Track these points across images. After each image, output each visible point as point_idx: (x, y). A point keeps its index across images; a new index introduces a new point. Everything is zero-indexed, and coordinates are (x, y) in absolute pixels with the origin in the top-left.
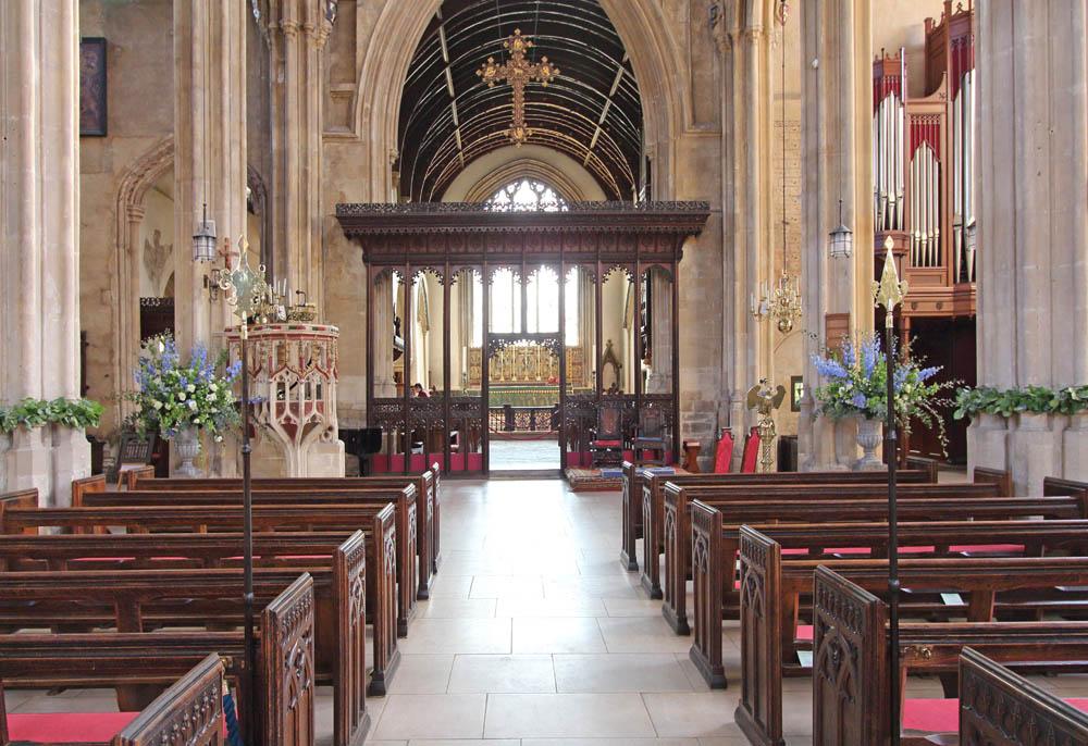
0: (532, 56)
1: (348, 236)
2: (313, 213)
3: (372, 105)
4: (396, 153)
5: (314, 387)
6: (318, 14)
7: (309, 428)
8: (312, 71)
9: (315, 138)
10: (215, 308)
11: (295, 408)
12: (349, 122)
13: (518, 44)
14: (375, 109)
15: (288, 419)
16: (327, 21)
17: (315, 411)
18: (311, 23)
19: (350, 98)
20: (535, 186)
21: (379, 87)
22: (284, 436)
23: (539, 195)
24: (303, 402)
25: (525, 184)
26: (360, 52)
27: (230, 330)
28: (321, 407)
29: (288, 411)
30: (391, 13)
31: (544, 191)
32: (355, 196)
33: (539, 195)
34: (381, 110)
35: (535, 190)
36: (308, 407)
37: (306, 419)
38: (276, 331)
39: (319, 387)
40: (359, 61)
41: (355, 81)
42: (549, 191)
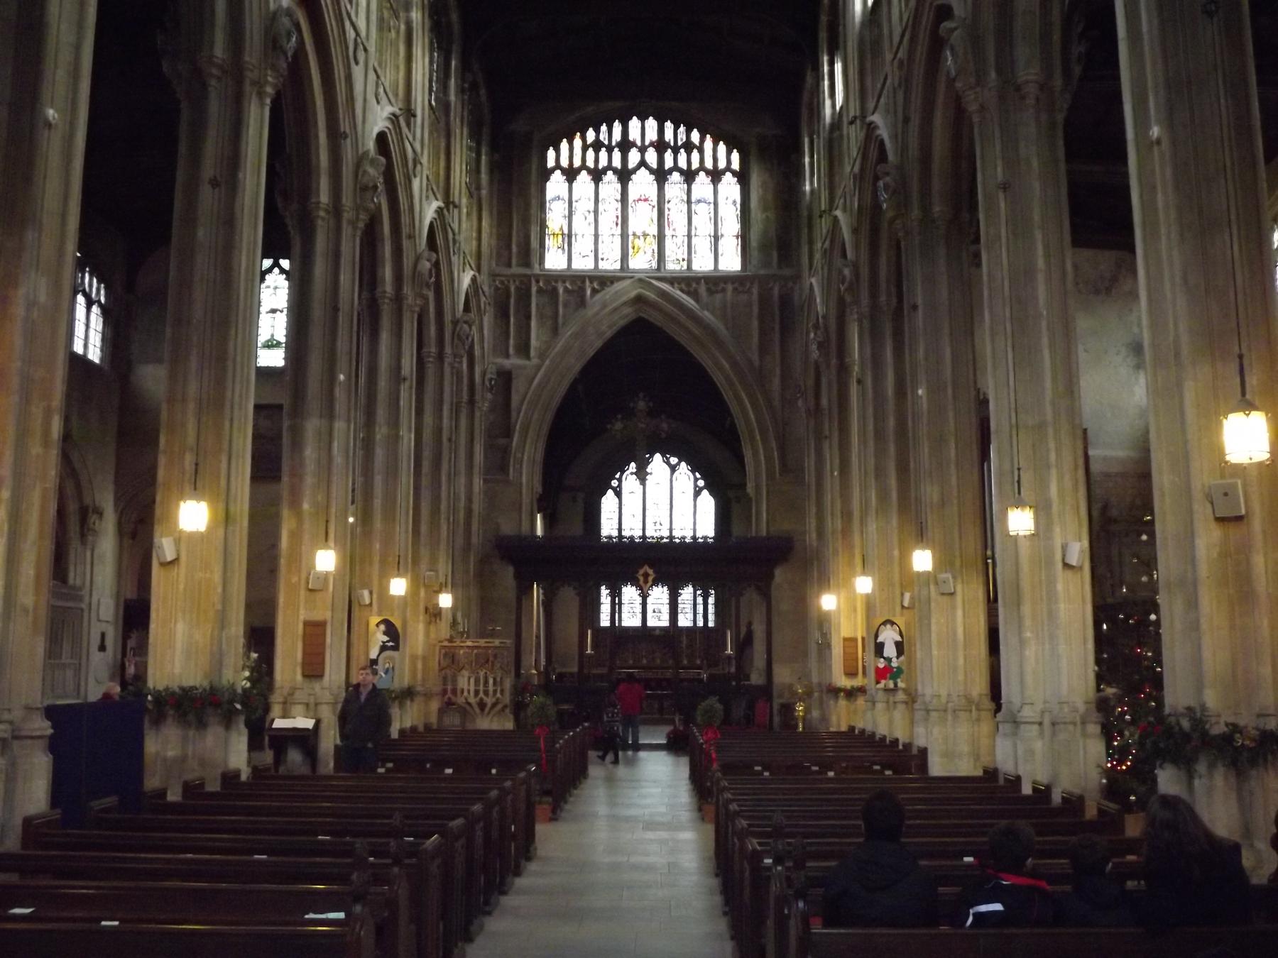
0: (651, 413)
1: (502, 558)
2: (474, 540)
3: (523, 454)
4: (540, 490)
5: (498, 679)
6: (483, 389)
7: (494, 705)
8: (477, 432)
9: (478, 483)
10: (432, 628)
11: (486, 693)
12: (504, 468)
13: (641, 405)
14: (526, 458)
15: (481, 699)
16: (489, 394)
17: (498, 695)
18: (478, 397)
19: (506, 451)
20: (668, 459)
21: (529, 441)
22: (477, 710)
23: (673, 469)
24: (491, 688)
25: (658, 457)
26: (514, 414)
27: (442, 642)
28: (502, 691)
29: (481, 695)
30: (539, 385)
31: (678, 464)
32: (507, 528)
33: (673, 469)
34: (529, 457)
35: (668, 463)
36: (495, 692)
37: (494, 700)
38: (476, 644)
39: (501, 678)
40: (513, 420)
41: (508, 434)
42: (683, 464)
